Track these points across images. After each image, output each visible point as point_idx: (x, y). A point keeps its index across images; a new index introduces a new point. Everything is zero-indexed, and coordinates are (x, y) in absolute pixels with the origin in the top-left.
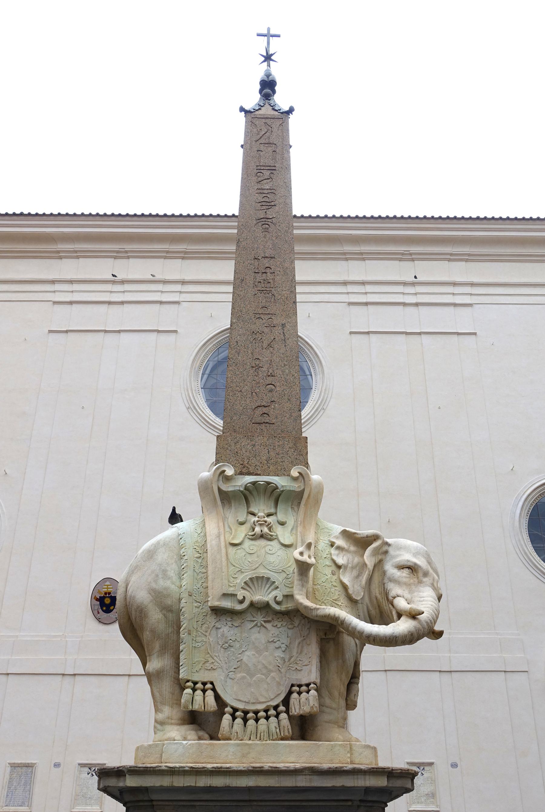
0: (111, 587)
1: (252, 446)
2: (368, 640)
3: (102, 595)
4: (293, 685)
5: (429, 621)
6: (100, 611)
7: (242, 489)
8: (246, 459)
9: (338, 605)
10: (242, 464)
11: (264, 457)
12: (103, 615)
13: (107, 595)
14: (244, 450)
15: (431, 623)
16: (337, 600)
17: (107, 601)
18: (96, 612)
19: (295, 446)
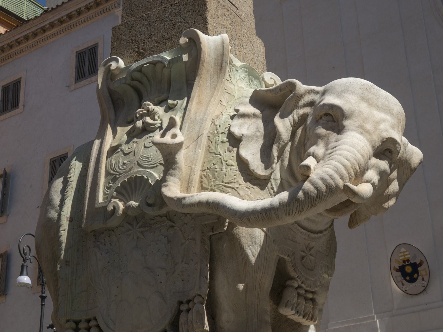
0: (407, 253)
1: (147, 26)
2: (244, 223)
3: (401, 265)
4: (181, 303)
5: (327, 177)
6: (404, 282)
7: (128, 82)
8: (141, 44)
9: (233, 188)
10: (137, 52)
11: (160, 33)
12: (409, 286)
13: (407, 263)
14: (138, 34)
15: (332, 179)
16: (232, 182)
17: (409, 269)
18: (400, 284)
19: (193, 8)
